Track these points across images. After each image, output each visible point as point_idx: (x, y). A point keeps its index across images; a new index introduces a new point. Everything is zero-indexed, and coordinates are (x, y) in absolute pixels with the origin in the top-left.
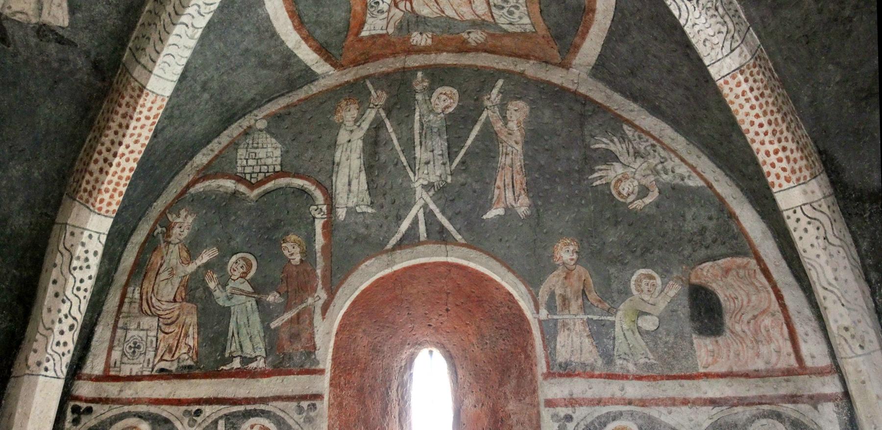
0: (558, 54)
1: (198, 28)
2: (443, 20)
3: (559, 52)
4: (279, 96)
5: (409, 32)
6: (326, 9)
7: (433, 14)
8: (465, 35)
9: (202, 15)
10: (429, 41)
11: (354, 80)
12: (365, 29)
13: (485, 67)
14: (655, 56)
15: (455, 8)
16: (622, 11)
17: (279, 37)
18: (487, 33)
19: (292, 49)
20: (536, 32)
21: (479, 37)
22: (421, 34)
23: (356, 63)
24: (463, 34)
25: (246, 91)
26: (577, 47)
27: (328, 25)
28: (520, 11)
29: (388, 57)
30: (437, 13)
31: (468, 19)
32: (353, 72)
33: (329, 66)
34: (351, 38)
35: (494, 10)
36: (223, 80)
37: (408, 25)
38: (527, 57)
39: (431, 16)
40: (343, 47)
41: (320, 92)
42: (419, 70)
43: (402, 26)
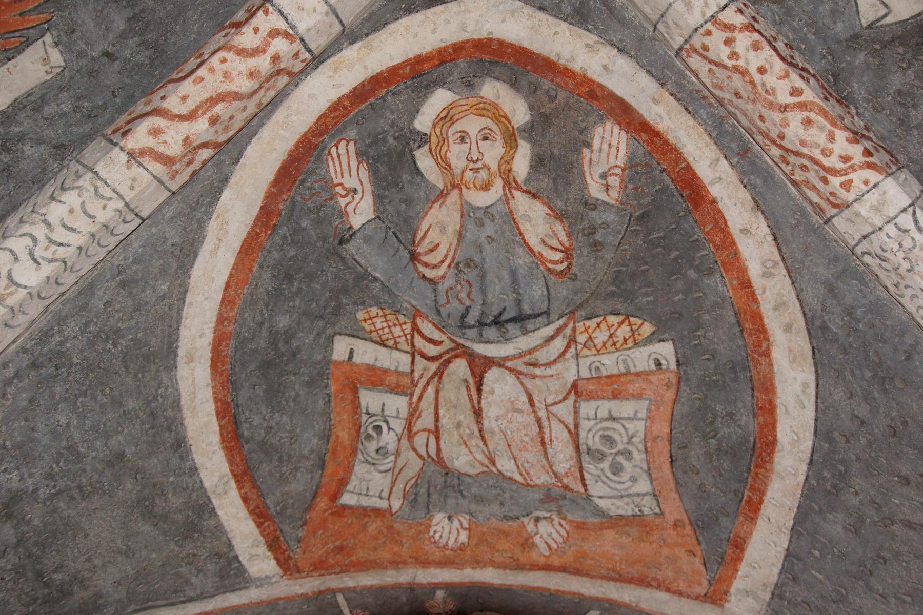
0: (702, 568)
1: (19, 285)
2: (491, 482)
3: (705, 564)
4: (166, 605)
5: (428, 511)
6: (285, 419)
7: (473, 466)
8: (530, 527)
9: (35, 260)
10: (464, 537)
11: (314, 593)
12: (350, 487)
13: (563, 592)
14: (909, 525)
15: (516, 453)
16: (830, 440)
17: (188, 452)
18: (571, 521)
19: (209, 493)
20: (662, 514)
21: (555, 535)
22: (450, 518)
23: (320, 567)
24: (525, 520)
25: (98, 562)
26: (739, 545)
27: (285, 458)
28: (633, 463)
29: (386, 568)
30: (482, 464)
31: (539, 482)
32: (317, 583)
33: (273, 562)
34: (322, 503)
35: (585, 458)
36: (54, 511)
37: (429, 495)
38: (643, 582)
39: (472, 472)
40: (305, 524)
41: (244, 604)
42: (440, 589)
43: (416, 494)
